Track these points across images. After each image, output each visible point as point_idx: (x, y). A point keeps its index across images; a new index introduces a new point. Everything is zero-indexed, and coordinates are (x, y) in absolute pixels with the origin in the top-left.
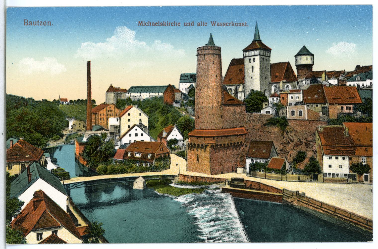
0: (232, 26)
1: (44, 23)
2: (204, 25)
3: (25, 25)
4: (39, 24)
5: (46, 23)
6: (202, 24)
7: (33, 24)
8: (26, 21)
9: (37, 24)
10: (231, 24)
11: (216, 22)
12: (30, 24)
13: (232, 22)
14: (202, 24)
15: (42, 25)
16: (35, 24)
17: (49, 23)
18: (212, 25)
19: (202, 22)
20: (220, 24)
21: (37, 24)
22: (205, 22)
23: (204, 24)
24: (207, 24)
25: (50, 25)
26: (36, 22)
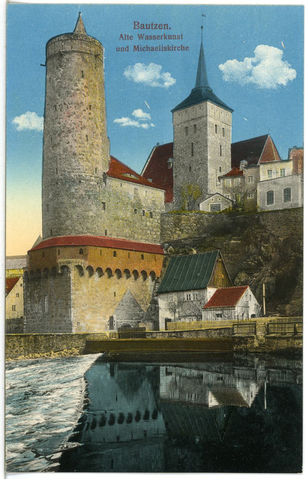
0: (164, 39)
1: (159, 26)
2: (129, 39)
3: (134, 28)
4: (154, 27)
5: (162, 26)
6: (127, 38)
7: (145, 27)
8: (136, 24)
9: (151, 27)
10: (163, 37)
11: (144, 34)
12: (142, 27)
13: (164, 34)
14: (127, 38)
15: (157, 28)
16: (148, 27)
17: (166, 26)
18: (140, 38)
19: (127, 35)
20: (149, 38)
21: (151, 27)
22: (129, 36)
23: (129, 37)
24: (132, 37)
25: (167, 28)
26: (149, 25)
